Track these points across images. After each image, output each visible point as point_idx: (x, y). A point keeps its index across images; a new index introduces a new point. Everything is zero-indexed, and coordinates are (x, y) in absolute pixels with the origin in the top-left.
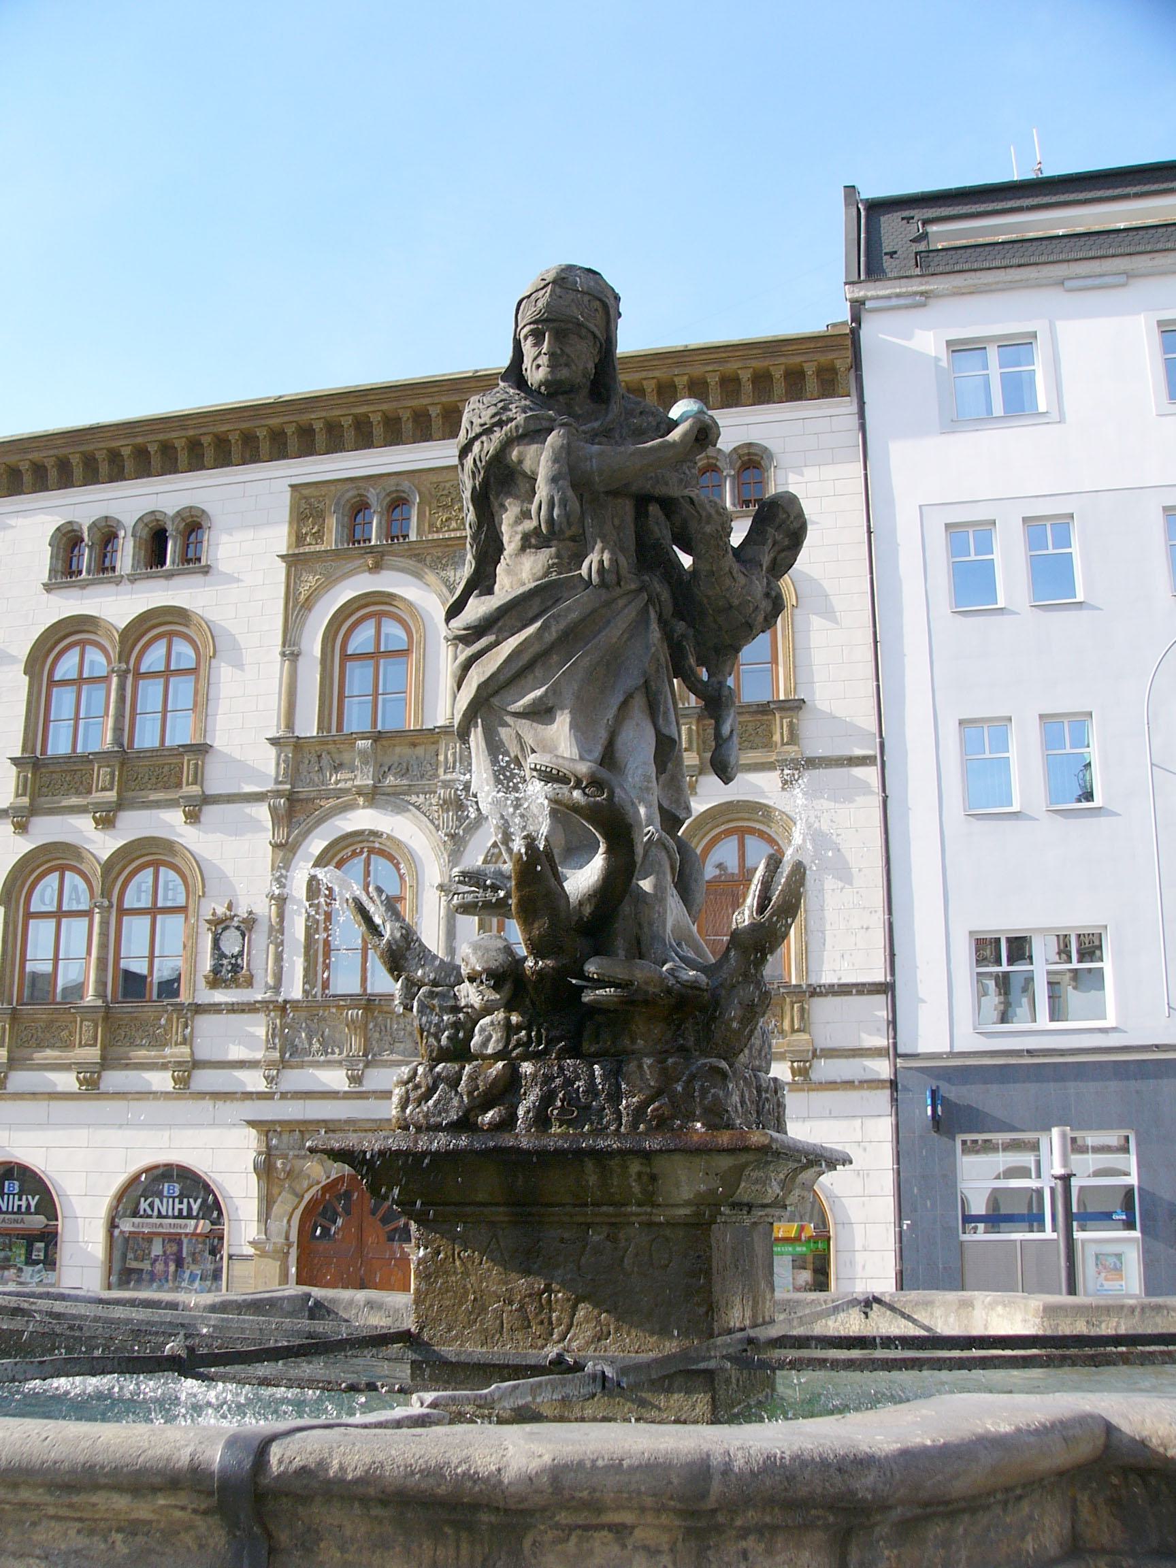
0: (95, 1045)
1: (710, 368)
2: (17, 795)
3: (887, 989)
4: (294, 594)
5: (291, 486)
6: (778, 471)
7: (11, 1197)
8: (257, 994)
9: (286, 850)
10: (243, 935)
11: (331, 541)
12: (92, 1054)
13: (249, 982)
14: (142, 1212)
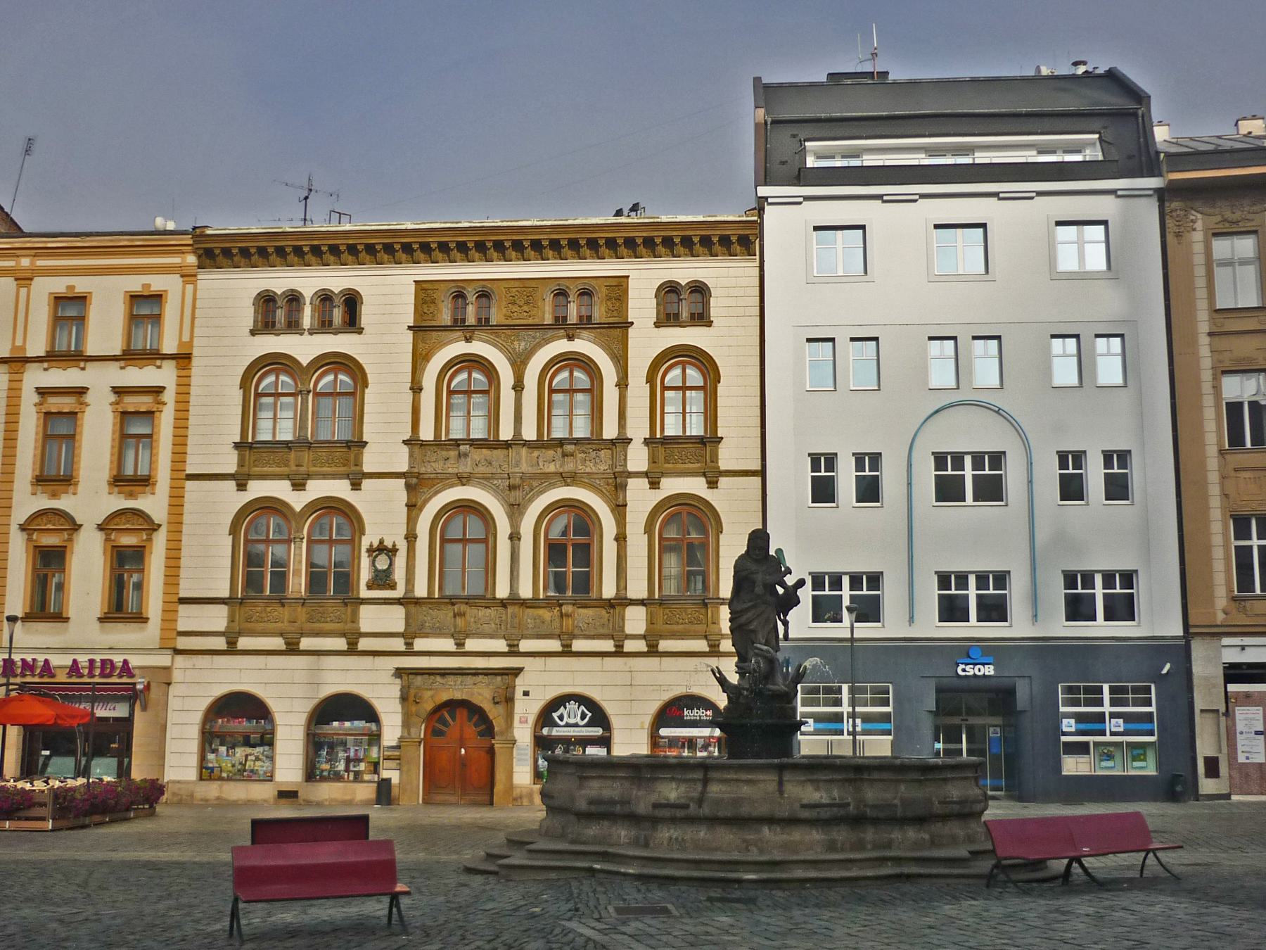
1: (675, 233)
5: (415, 281)
8: (399, 593)
9: (413, 508)
10: (391, 560)
13: (393, 587)
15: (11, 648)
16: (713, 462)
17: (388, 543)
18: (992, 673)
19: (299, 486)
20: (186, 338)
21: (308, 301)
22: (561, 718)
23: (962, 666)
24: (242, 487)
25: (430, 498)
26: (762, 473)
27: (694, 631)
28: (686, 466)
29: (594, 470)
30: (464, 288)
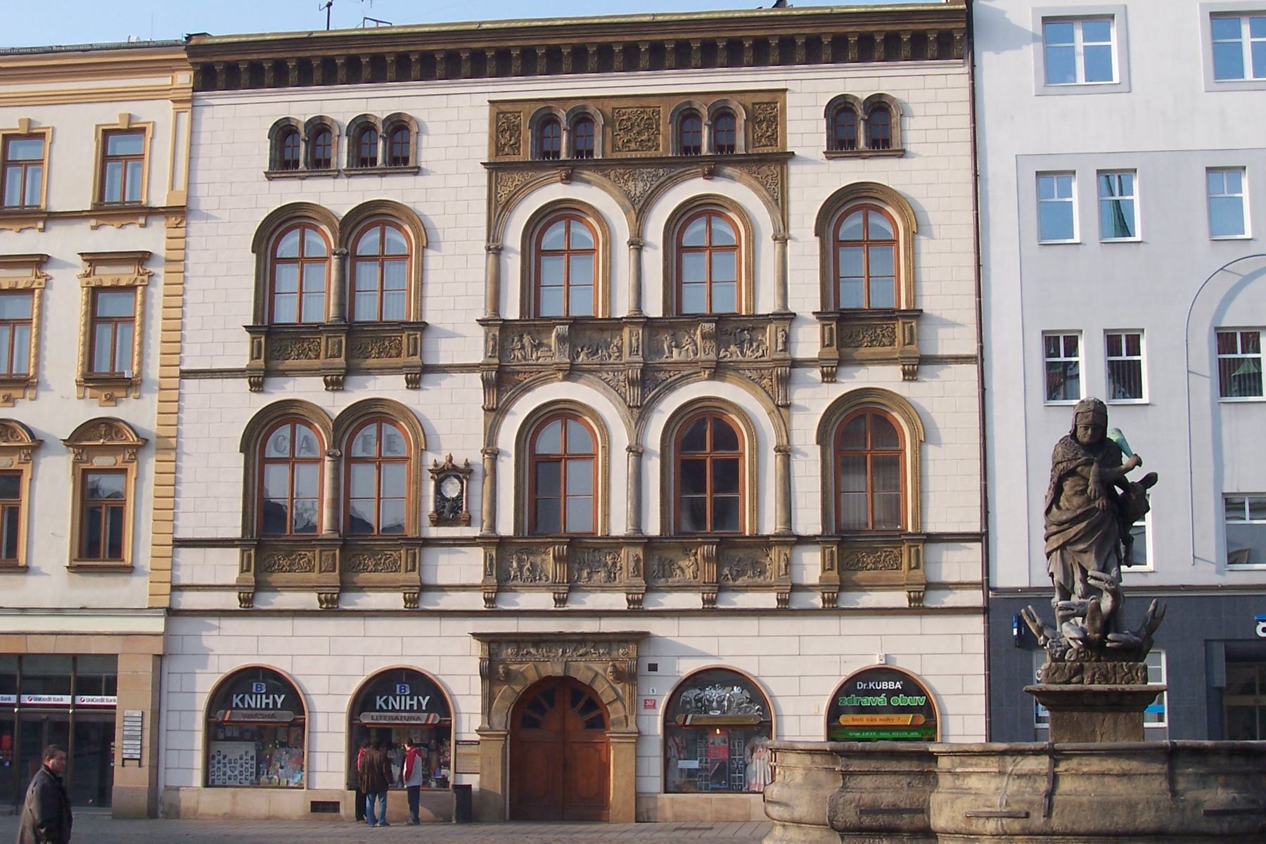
0: (334, 571)
2: (252, 358)
3: (983, 537)
4: (496, 196)
5: (490, 101)
6: (903, 118)
7: (259, 696)
9: (496, 413)
11: (526, 153)
12: (334, 578)
13: (468, 522)
14: (378, 707)
17: (459, 461)
20: (181, 184)
27: (888, 579)
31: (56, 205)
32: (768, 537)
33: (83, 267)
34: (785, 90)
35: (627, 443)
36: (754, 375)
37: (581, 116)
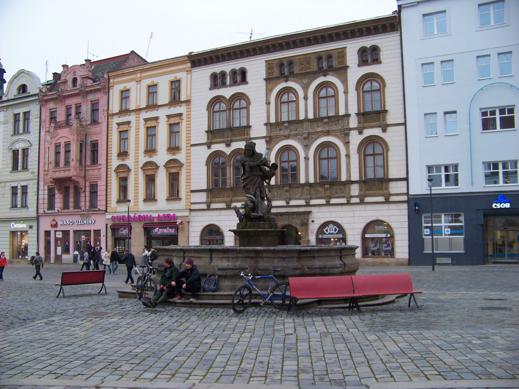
1: (363, 26)
3: (406, 179)
15: (129, 212)
16: (384, 121)
18: (509, 207)
19: (228, 145)
20: (189, 94)
21: (228, 74)
22: (327, 231)
23: (495, 204)
24: (209, 147)
25: (275, 146)
26: (405, 124)
28: (373, 123)
29: (336, 129)
30: (283, 61)
31: (159, 103)
32: (344, 182)
33: (166, 119)
34: (346, 47)
35: (304, 156)
36: (339, 133)
37: (291, 62)
